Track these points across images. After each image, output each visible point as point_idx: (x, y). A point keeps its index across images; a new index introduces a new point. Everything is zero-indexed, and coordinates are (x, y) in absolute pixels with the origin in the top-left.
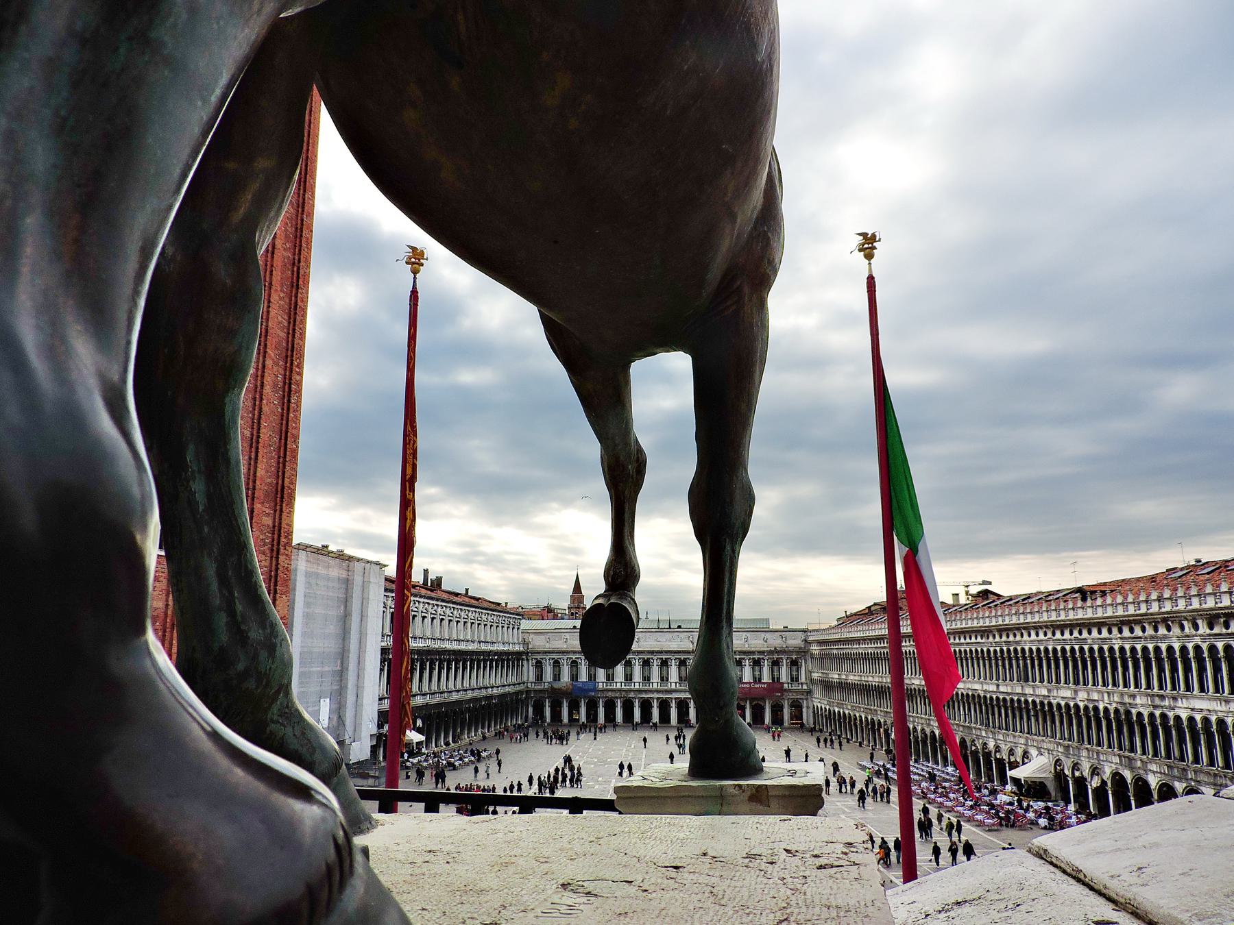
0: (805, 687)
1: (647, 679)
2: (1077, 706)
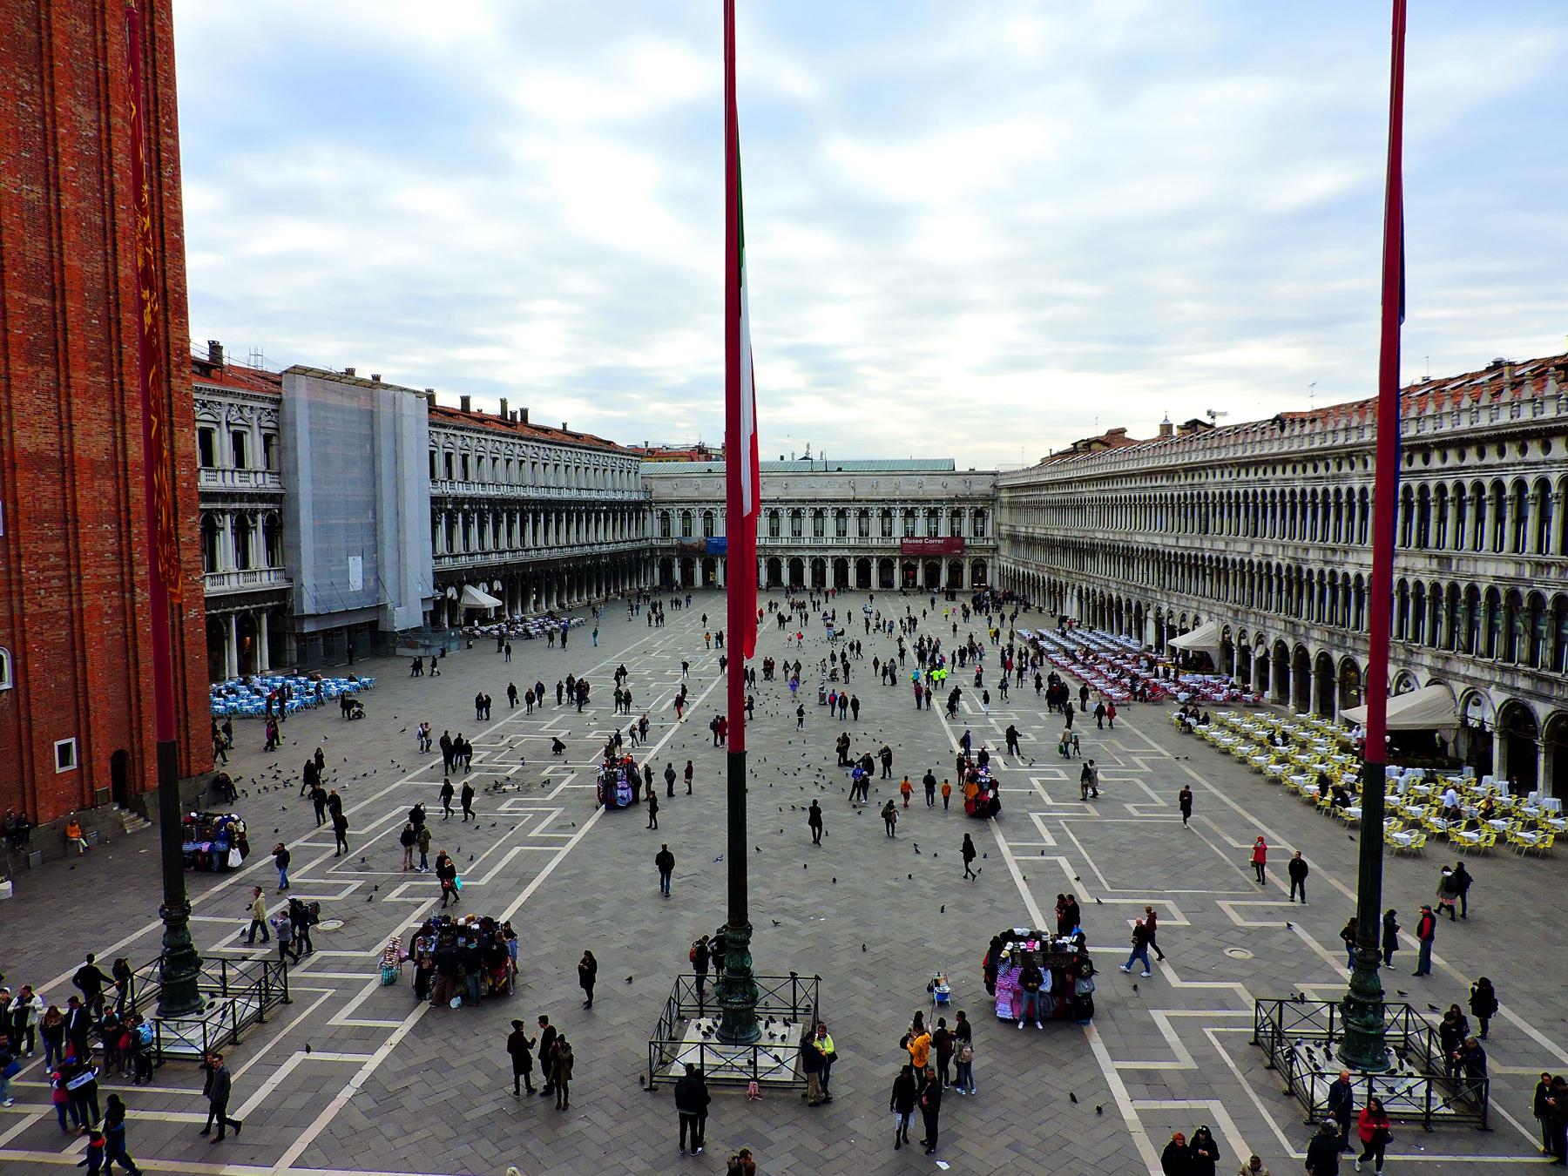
0: (991, 543)
1: (797, 533)
2: (1251, 562)
